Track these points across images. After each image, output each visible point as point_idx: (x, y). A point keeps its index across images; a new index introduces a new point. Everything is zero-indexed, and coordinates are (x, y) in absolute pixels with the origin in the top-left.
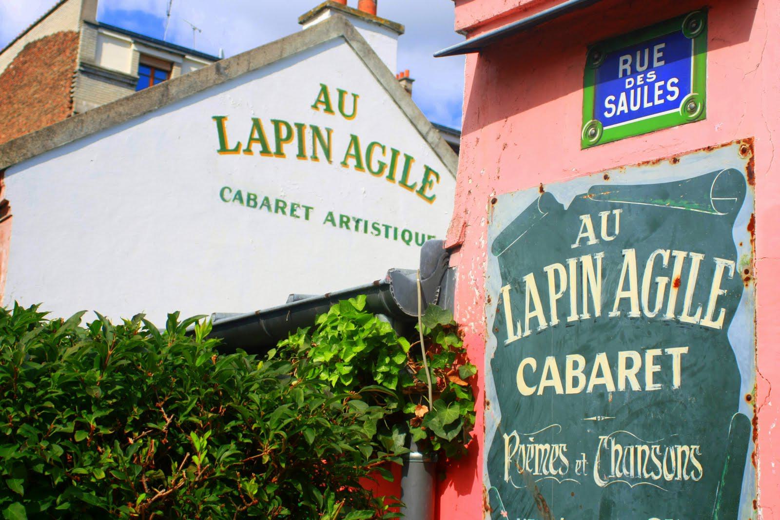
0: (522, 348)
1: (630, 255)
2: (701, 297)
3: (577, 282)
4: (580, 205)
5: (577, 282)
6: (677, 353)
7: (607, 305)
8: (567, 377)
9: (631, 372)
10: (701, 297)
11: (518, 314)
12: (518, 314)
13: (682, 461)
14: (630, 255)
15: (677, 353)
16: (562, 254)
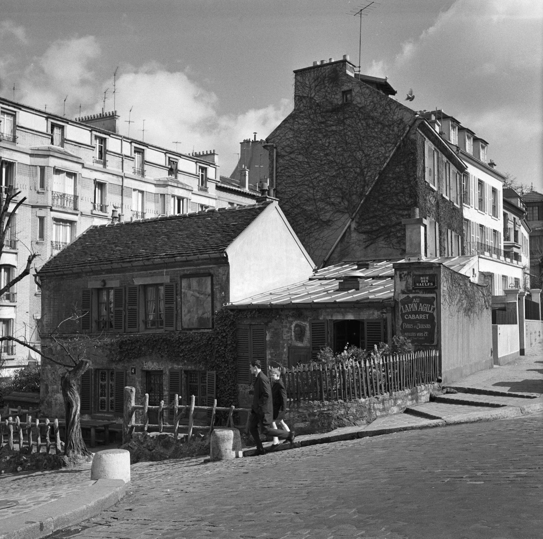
0: (405, 313)
1: (421, 304)
2: (430, 309)
3: (414, 306)
4: (413, 297)
5: (414, 306)
6: (427, 315)
7: (418, 309)
8: (413, 317)
9: (422, 317)
10: (430, 309)
11: (405, 308)
12: (405, 308)
13: (428, 326)
14: (421, 304)
15: (427, 315)
16: (411, 303)
